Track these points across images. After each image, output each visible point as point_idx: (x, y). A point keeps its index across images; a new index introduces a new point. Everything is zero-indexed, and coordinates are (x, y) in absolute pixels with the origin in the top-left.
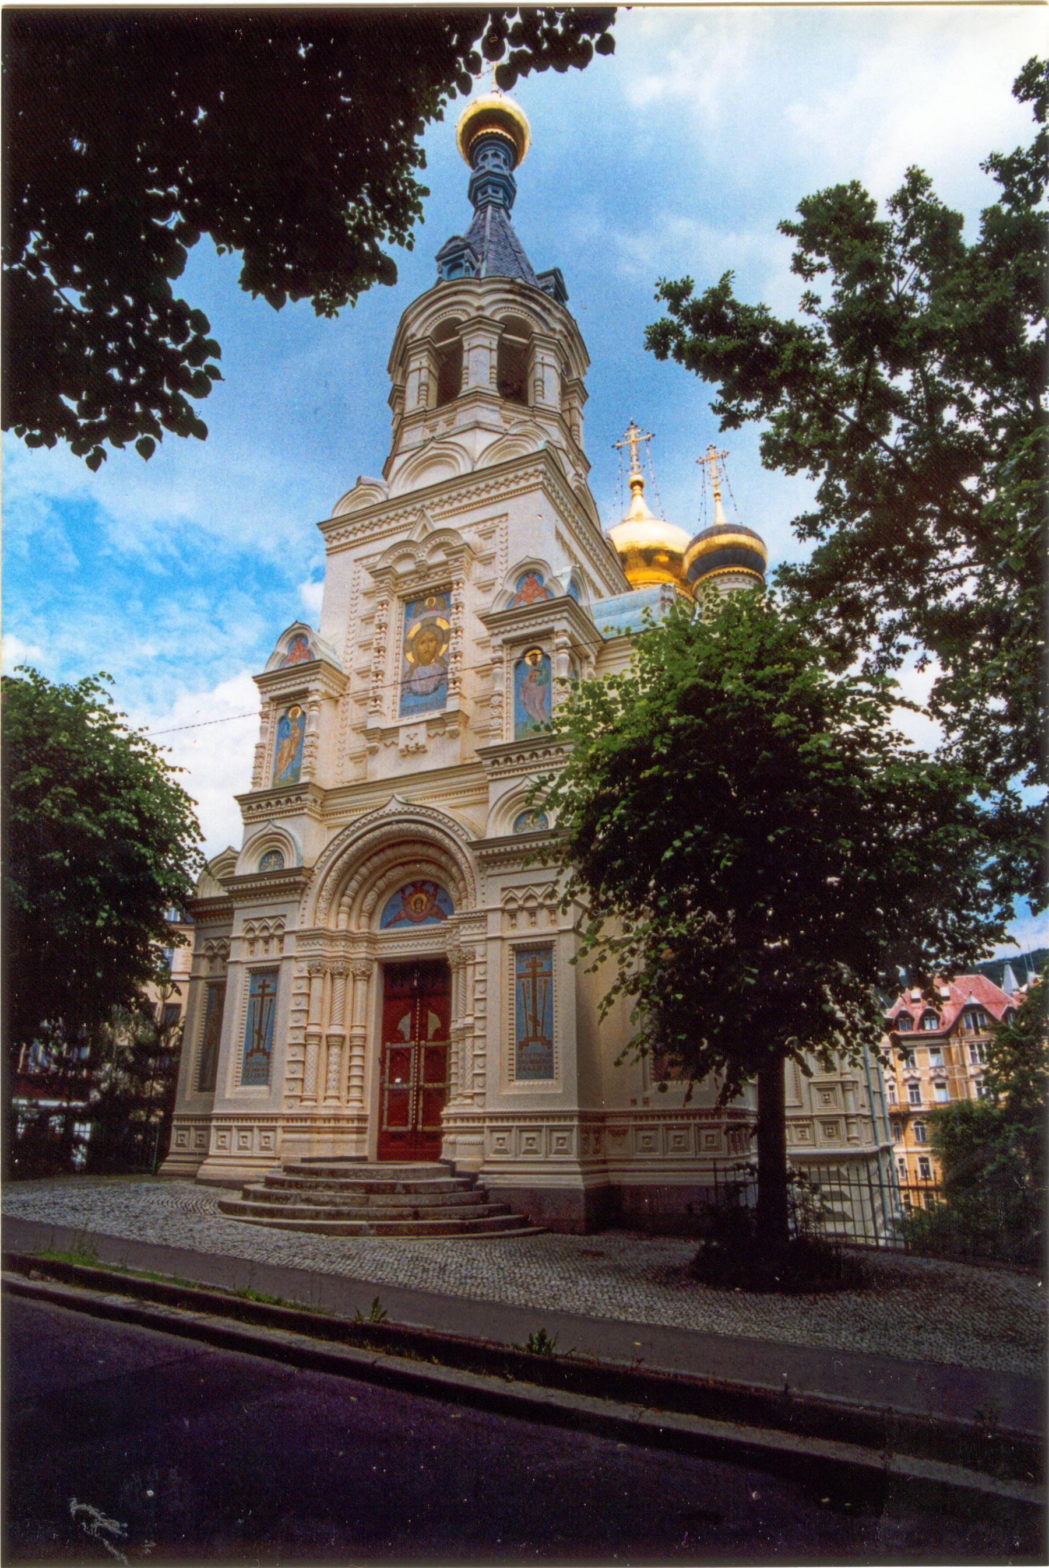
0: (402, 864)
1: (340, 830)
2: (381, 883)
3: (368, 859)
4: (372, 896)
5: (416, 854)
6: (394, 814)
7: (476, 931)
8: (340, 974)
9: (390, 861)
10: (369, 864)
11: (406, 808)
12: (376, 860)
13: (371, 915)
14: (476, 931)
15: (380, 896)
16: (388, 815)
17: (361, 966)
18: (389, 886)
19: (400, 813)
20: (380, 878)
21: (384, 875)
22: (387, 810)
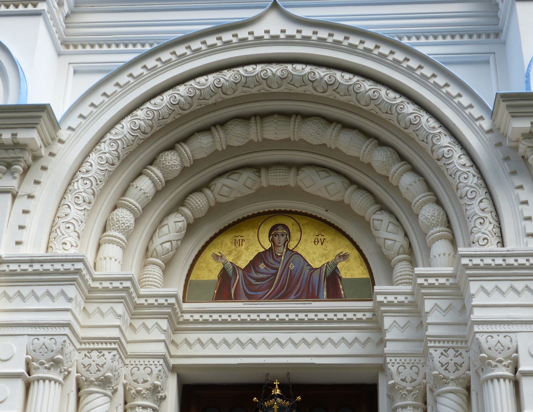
0: (257, 168)
1: (97, 78)
2: (199, 202)
3: (185, 139)
4: (176, 223)
5: (302, 145)
6: (275, 40)
7: (512, 299)
8: (105, 382)
9: (231, 151)
10: (185, 149)
11: (307, 32)
12: (203, 144)
13: (168, 265)
14: (512, 299)
15: (191, 228)
16: (259, 41)
17: (150, 373)
18: (214, 210)
19: (290, 40)
20: (198, 189)
21: (207, 185)
22: (258, 30)
